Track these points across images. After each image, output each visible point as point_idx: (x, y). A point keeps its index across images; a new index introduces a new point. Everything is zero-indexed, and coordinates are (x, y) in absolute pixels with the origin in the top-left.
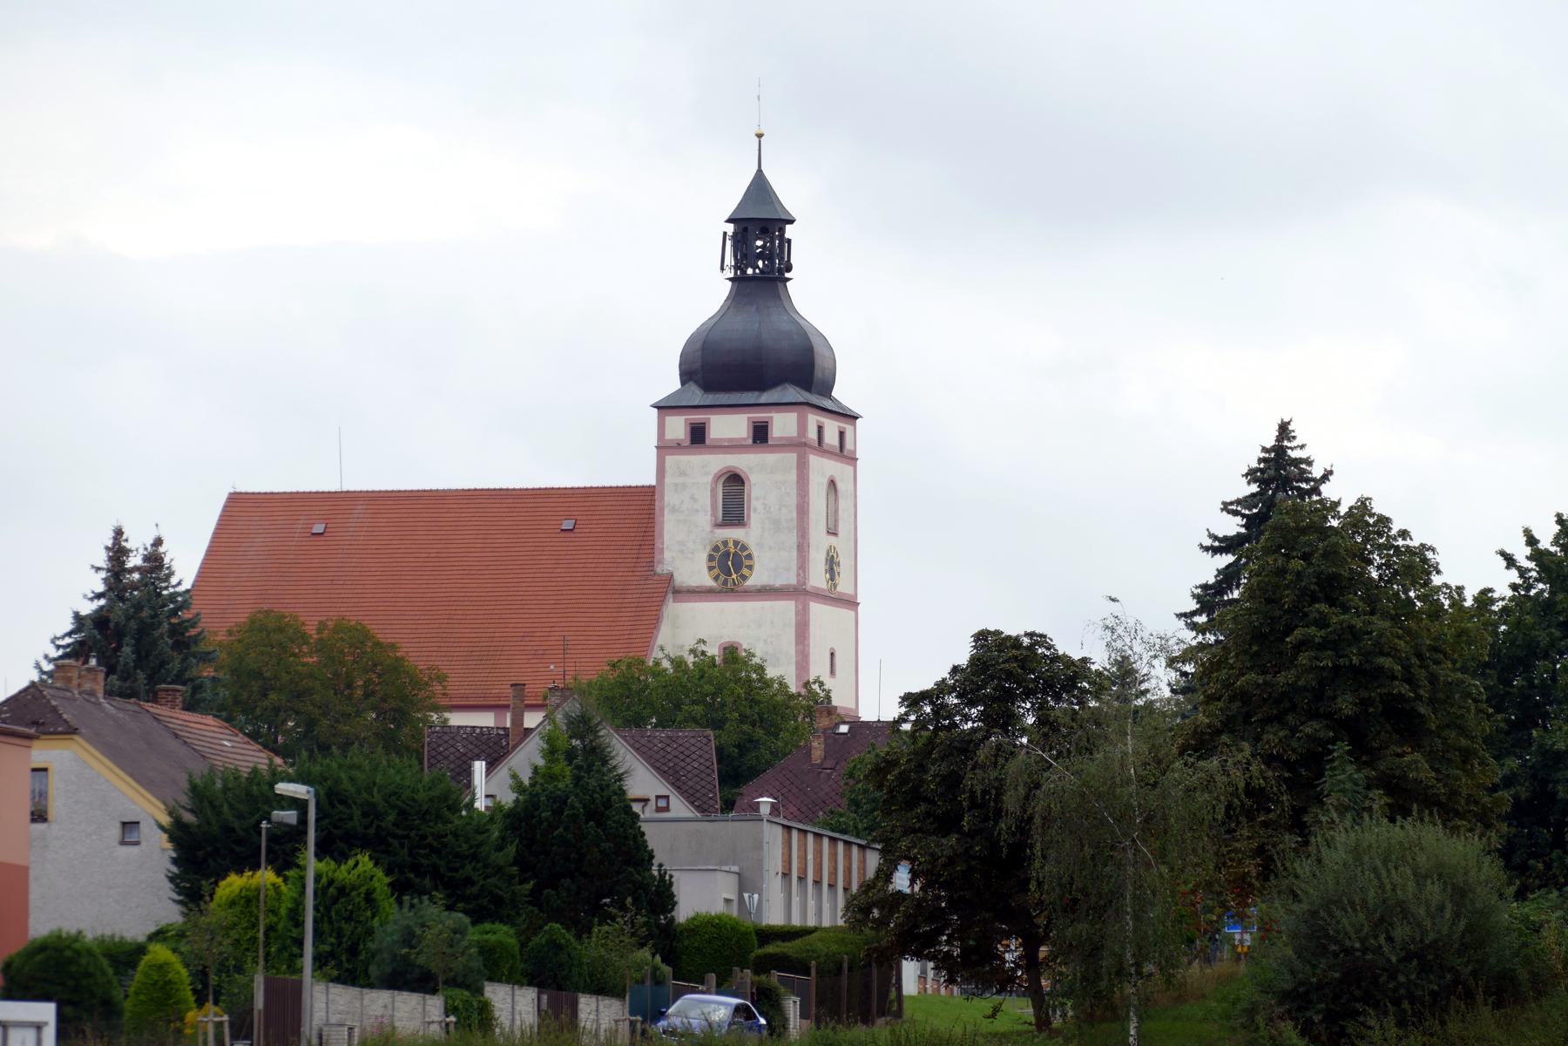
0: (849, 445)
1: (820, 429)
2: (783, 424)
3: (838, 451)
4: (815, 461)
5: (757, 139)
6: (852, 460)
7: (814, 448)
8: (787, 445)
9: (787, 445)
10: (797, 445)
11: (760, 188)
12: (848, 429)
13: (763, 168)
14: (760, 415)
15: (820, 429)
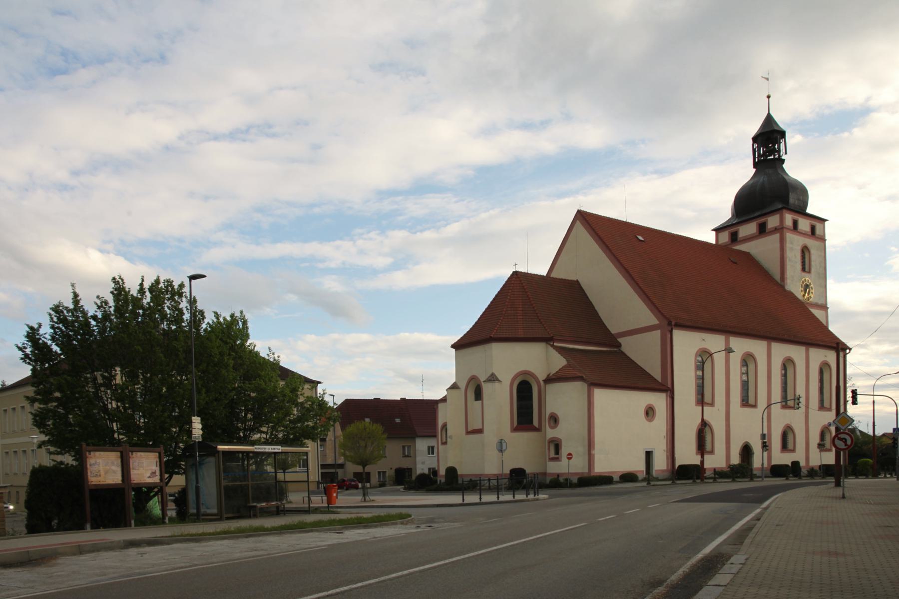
0: (818, 232)
1: (795, 223)
2: (773, 221)
3: (810, 234)
4: (789, 236)
5: (767, 99)
6: (823, 239)
7: (791, 230)
8: (776, 230)
9: (776, 230)
10: (780, 229)
11: (769, 120)
12: (818, 226)
13: (770, 112)
14: (761, 220)
15: (795, 223)
